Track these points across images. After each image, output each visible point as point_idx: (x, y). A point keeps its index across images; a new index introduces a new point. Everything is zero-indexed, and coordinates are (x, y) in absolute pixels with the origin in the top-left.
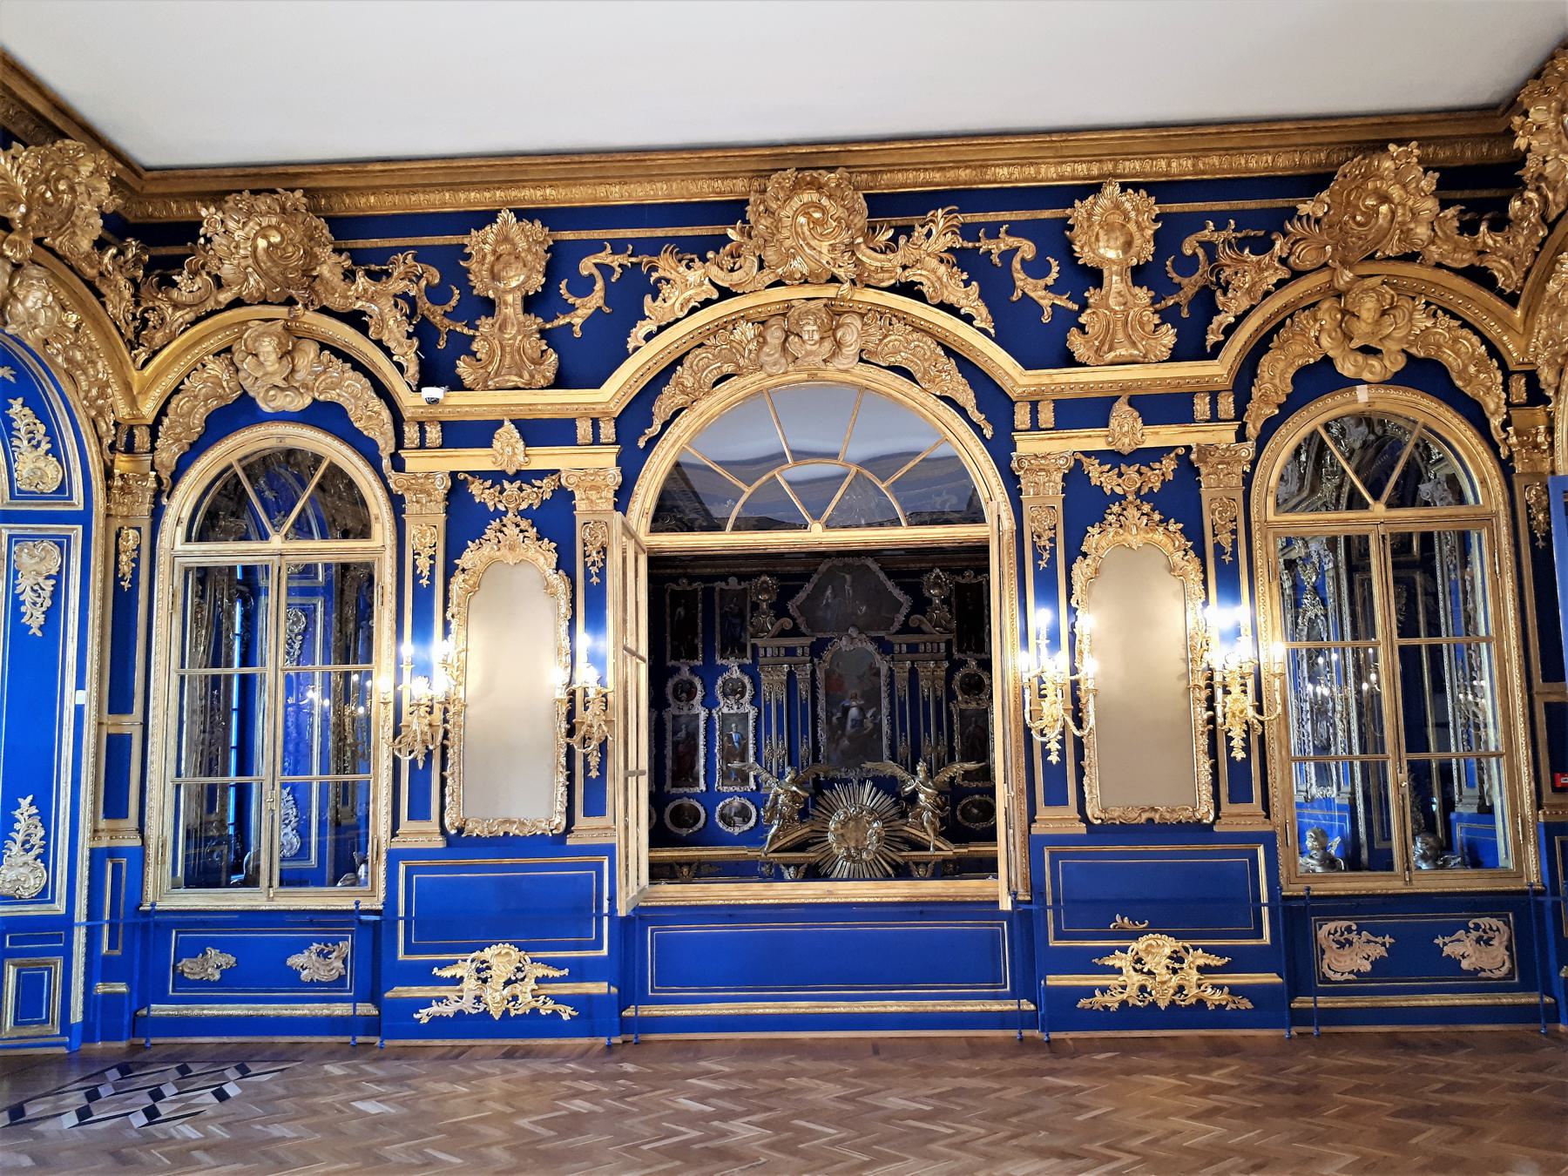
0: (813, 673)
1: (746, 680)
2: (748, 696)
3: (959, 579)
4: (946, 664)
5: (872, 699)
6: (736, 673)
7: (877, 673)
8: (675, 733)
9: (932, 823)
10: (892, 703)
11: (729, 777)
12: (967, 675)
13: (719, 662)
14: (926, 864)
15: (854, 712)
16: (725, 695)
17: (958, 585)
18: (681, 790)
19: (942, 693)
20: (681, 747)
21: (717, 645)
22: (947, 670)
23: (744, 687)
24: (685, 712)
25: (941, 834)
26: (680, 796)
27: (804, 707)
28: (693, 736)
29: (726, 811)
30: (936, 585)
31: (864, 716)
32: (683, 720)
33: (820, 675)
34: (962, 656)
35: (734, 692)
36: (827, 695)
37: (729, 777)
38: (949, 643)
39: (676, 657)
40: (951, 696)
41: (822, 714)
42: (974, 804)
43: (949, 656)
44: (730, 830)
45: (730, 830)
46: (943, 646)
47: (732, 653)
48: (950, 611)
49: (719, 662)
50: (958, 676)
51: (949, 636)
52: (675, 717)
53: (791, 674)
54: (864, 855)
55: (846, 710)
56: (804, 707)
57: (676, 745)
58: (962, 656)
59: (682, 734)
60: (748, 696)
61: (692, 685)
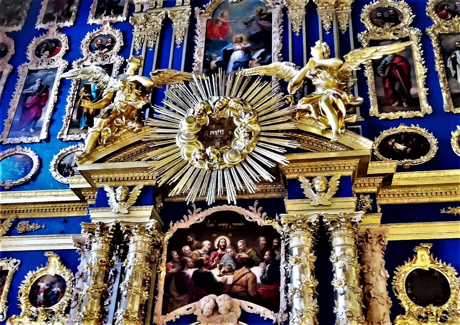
0: (193, 21)
1: (117, 34)
2: (117, 47)
5: (261, 39)
6: (107, 30)
7: (269, 17)
8: (26, 86)
9: (334, 106)
10: (284, 41)
11: (78, 127)
12: (379, 9)
13: (91, 21)
15: (237, 55)
16: (91, 49)
18: (17, 140)
19: (345, 23)
20: (30, 100)
21: (93, 7)
23: (114, 41)
24: (44, 66)
26: (14, 145)
27: (178, 52)
28: (45, 89)
29: (66, 161)
31: (250, 58)
32: (40, 74)
33: (201, 25)
35: (102, 47)
36: (208, 41)
37: (78, 127)
39: (48, 18)
41: (198, 58)
42: (398, 138)
44: (65, 180)
45: (65, 180)
47: (108, 14)
49: (91, 21)
52: (30, 72)
53: (167, 23)
54: (227, 158)
55: (228, 54)
56: (178, 52)
57: (24, 97)
59: (36, 87)
60: (117, 47)
61: (57, 43)
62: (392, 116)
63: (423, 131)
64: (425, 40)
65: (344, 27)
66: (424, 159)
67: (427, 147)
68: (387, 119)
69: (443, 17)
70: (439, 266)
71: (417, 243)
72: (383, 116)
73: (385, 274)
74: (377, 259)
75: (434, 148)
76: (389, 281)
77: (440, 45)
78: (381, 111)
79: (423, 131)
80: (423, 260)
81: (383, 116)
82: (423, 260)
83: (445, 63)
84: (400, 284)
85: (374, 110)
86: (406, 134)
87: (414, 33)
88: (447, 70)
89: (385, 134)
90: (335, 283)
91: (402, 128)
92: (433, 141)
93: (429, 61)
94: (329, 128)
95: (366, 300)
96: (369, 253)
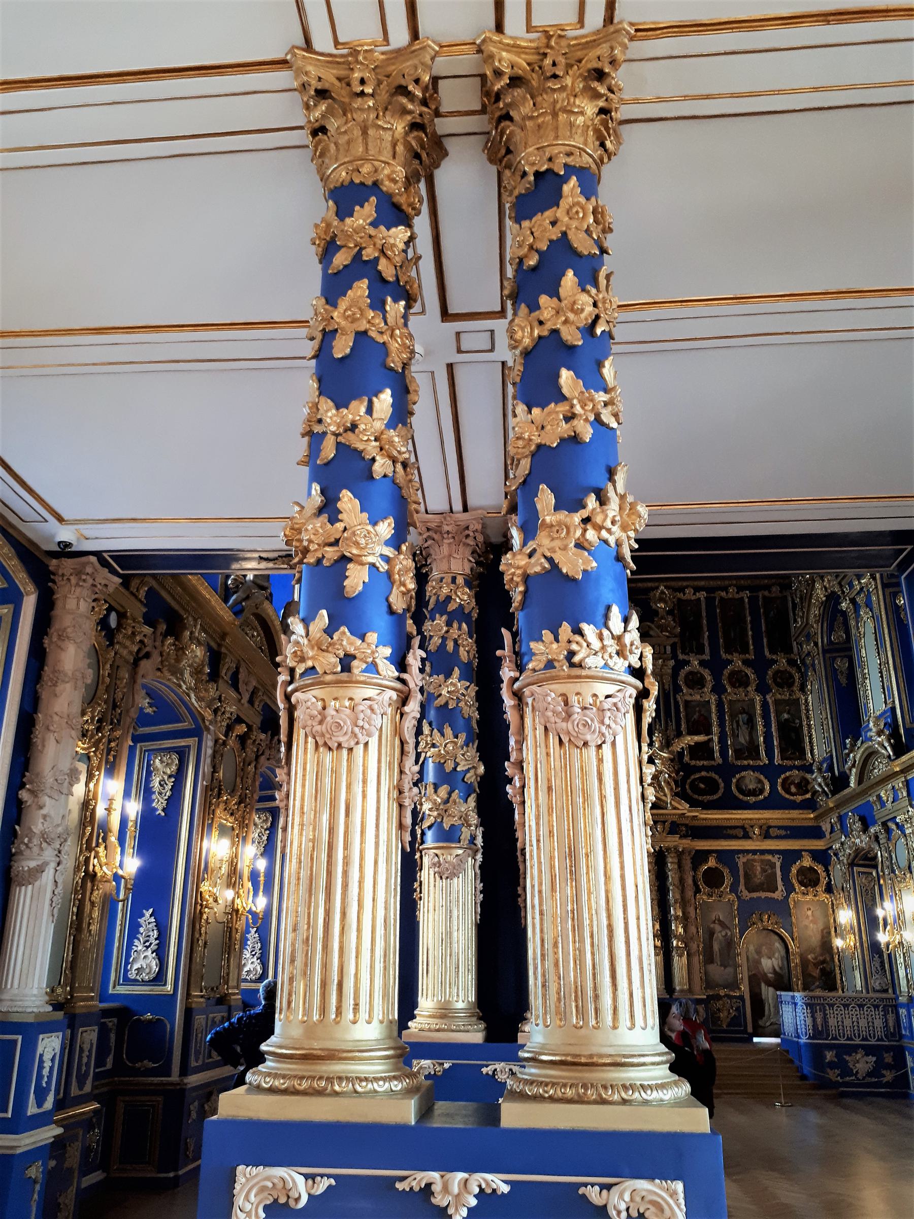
3: (680, 595)
4: (672, 663)
12: (691, 673)
14: (664, 822)
17: (679, 599)
22: (674, 668)
25: (676, 794)
30: (661, 600)
34: (685, 657)
38: (673, 646)
40: (677, 689)
42: (702, 779)
43: (674, 656)
46: (669, 648)
48: (674, 620)
50: (683, 673)
51: (676, 640)
58: (685, 657)
62: (700, 763)
63: (717, 777)
64: (720, 705)
65: (666, 687)
66: (715, 797)
67: (717, 788)
68: (694, 766)
69: (733, 685)
70: (720, 867)
71: (709, 852)
72: (693, 763)
73: (692, 873)
74: (688, 864)
75: (721, 791)
76: (694, 877)
77: (730, 709)
78: (691, 759)
79: (717, 777)
80: (712, 863)
81: (693, 763)
82: (712, 863)
83: (732, 722)
84: (700, 875)
85: (686, 759)
86: (706, 777)
87: (713, 698)
88: (733, 729)
89: (693, 777)
90: (668, 884)
91: (704, 774)
92: (722, 785)
93: (722, 725)
94: (665, 795)
95: (683, 892)
96: (684, 862)
